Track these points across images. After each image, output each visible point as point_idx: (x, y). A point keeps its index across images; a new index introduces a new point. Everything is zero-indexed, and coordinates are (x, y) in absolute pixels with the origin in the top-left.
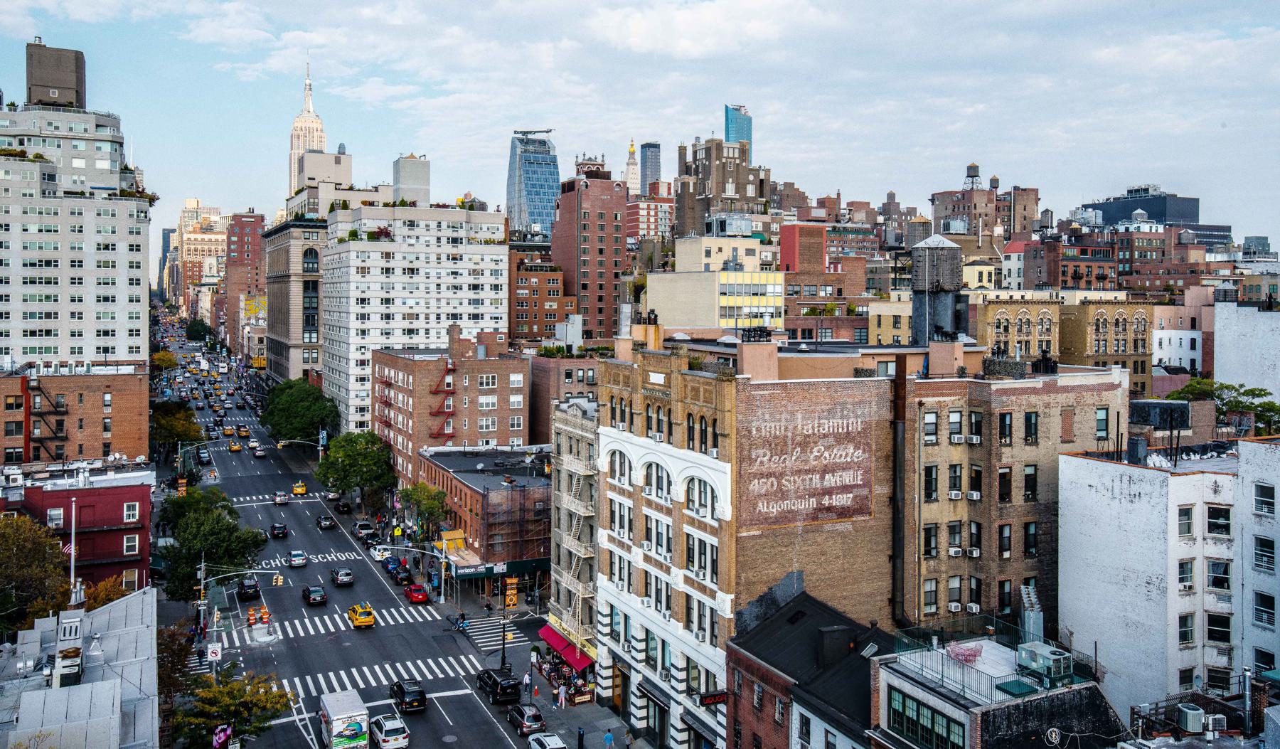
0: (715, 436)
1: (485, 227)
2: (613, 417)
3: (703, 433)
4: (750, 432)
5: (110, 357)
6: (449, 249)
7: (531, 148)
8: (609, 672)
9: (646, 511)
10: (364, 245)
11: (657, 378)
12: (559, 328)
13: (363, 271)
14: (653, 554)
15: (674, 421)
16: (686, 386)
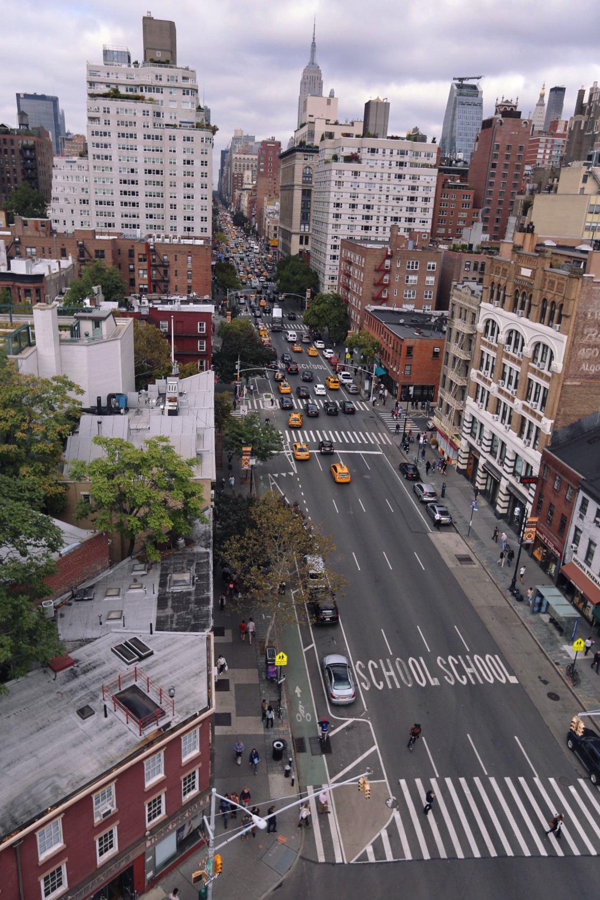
0: (560, 316)
1: (423, 154)
2: (492, 297)
3: (552, 313)
4: (586, 315)
5: (191, 234)
6: (397, 170)
7: (464, 91)
8: (467, 456)
9: (505, 361)
10: (341, 165)
11: (526, 272)
12: (465, 232)
13: (339, 183)
14: (505, 389)
15: (533, 302)
16: (545, 280)
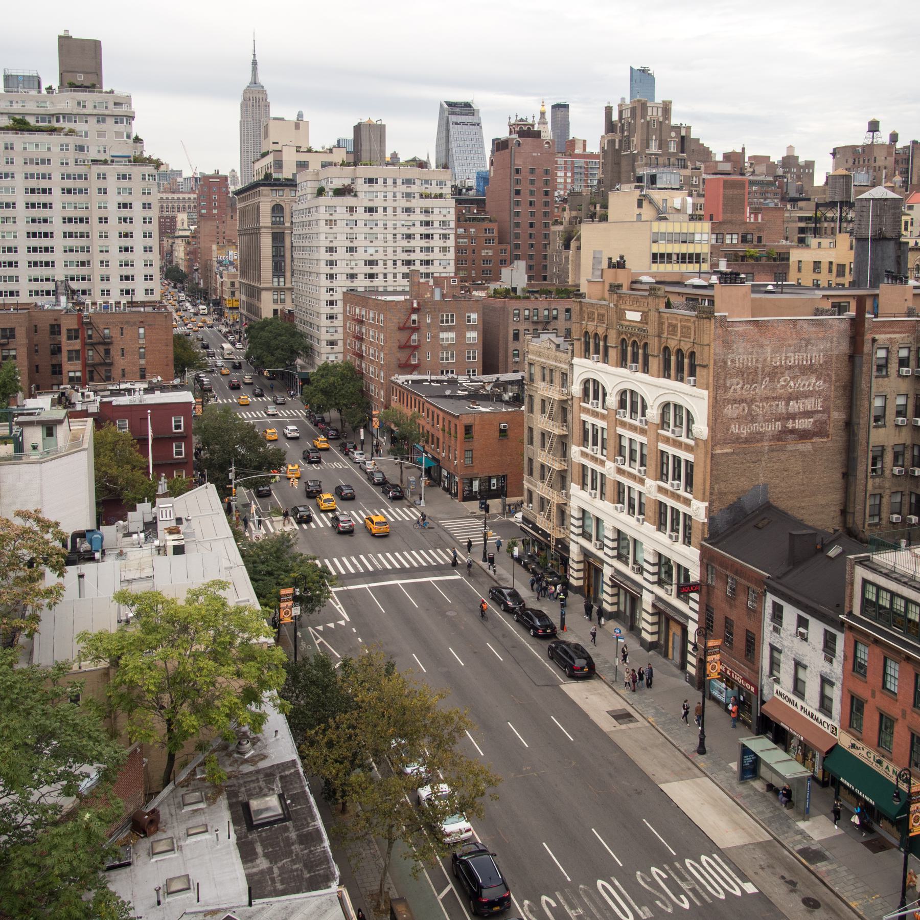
4: (726, 363)
9: (620, 430)
16: (663, 323)
